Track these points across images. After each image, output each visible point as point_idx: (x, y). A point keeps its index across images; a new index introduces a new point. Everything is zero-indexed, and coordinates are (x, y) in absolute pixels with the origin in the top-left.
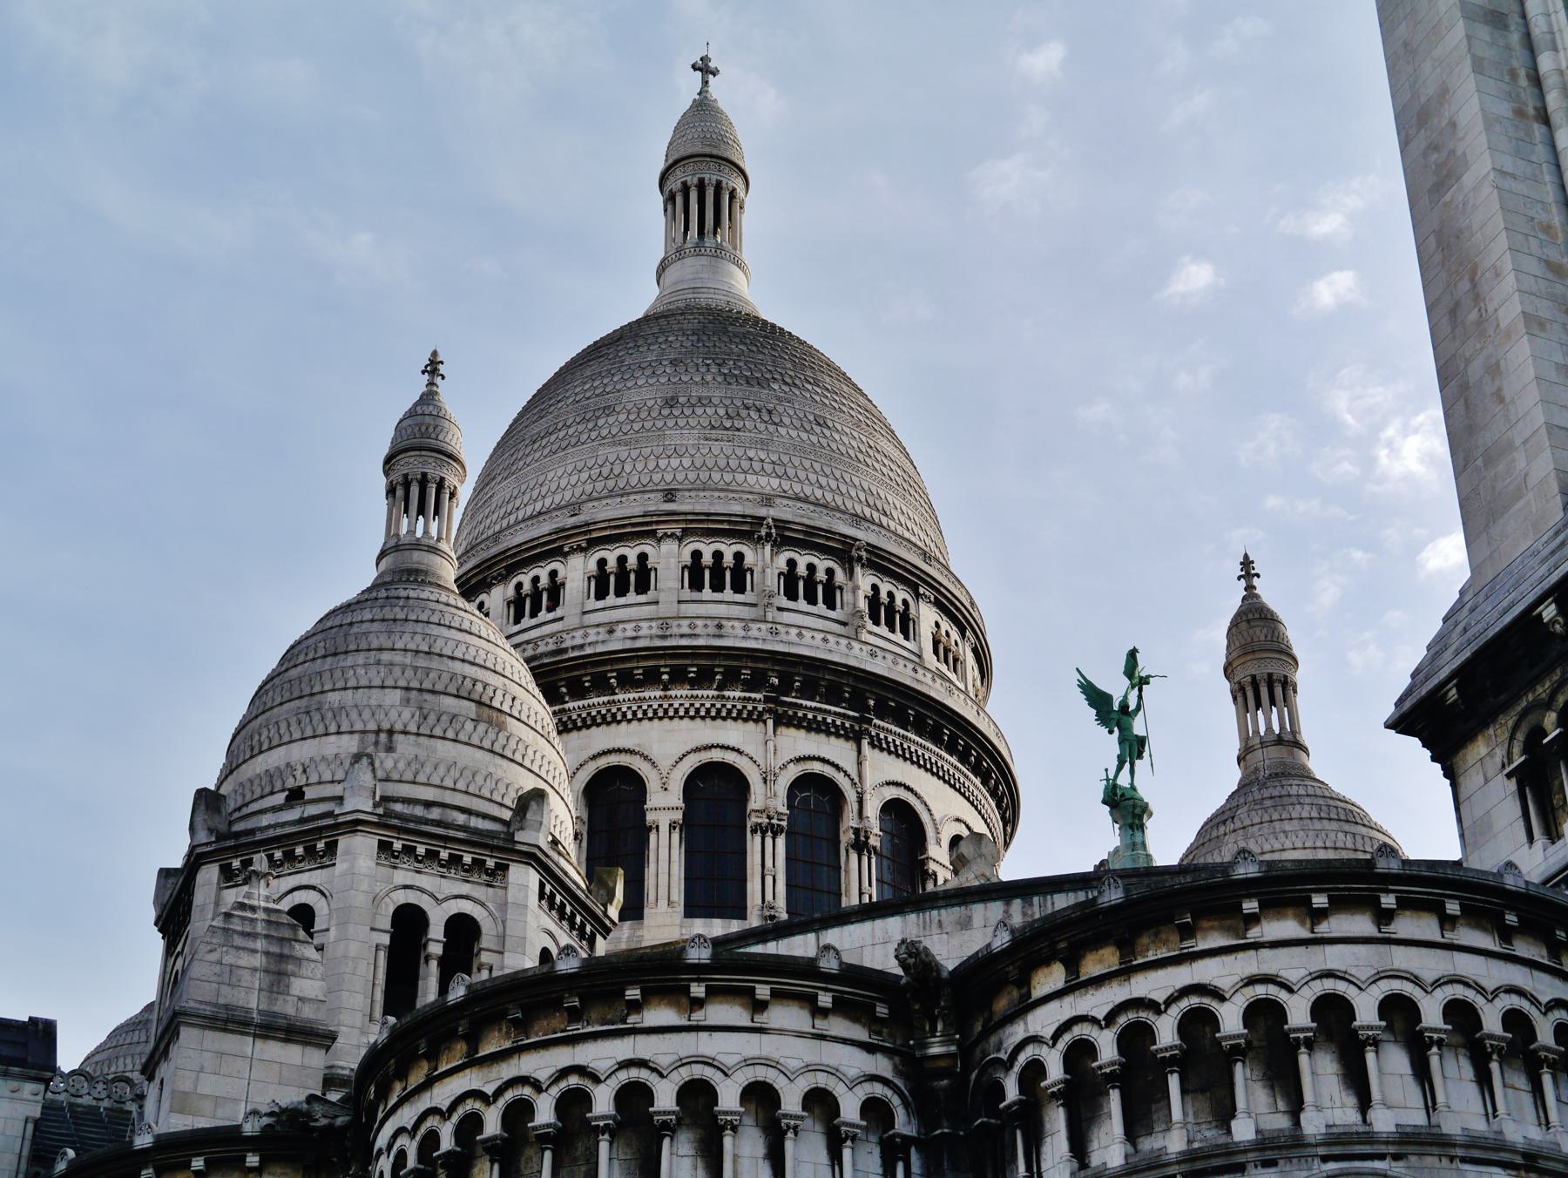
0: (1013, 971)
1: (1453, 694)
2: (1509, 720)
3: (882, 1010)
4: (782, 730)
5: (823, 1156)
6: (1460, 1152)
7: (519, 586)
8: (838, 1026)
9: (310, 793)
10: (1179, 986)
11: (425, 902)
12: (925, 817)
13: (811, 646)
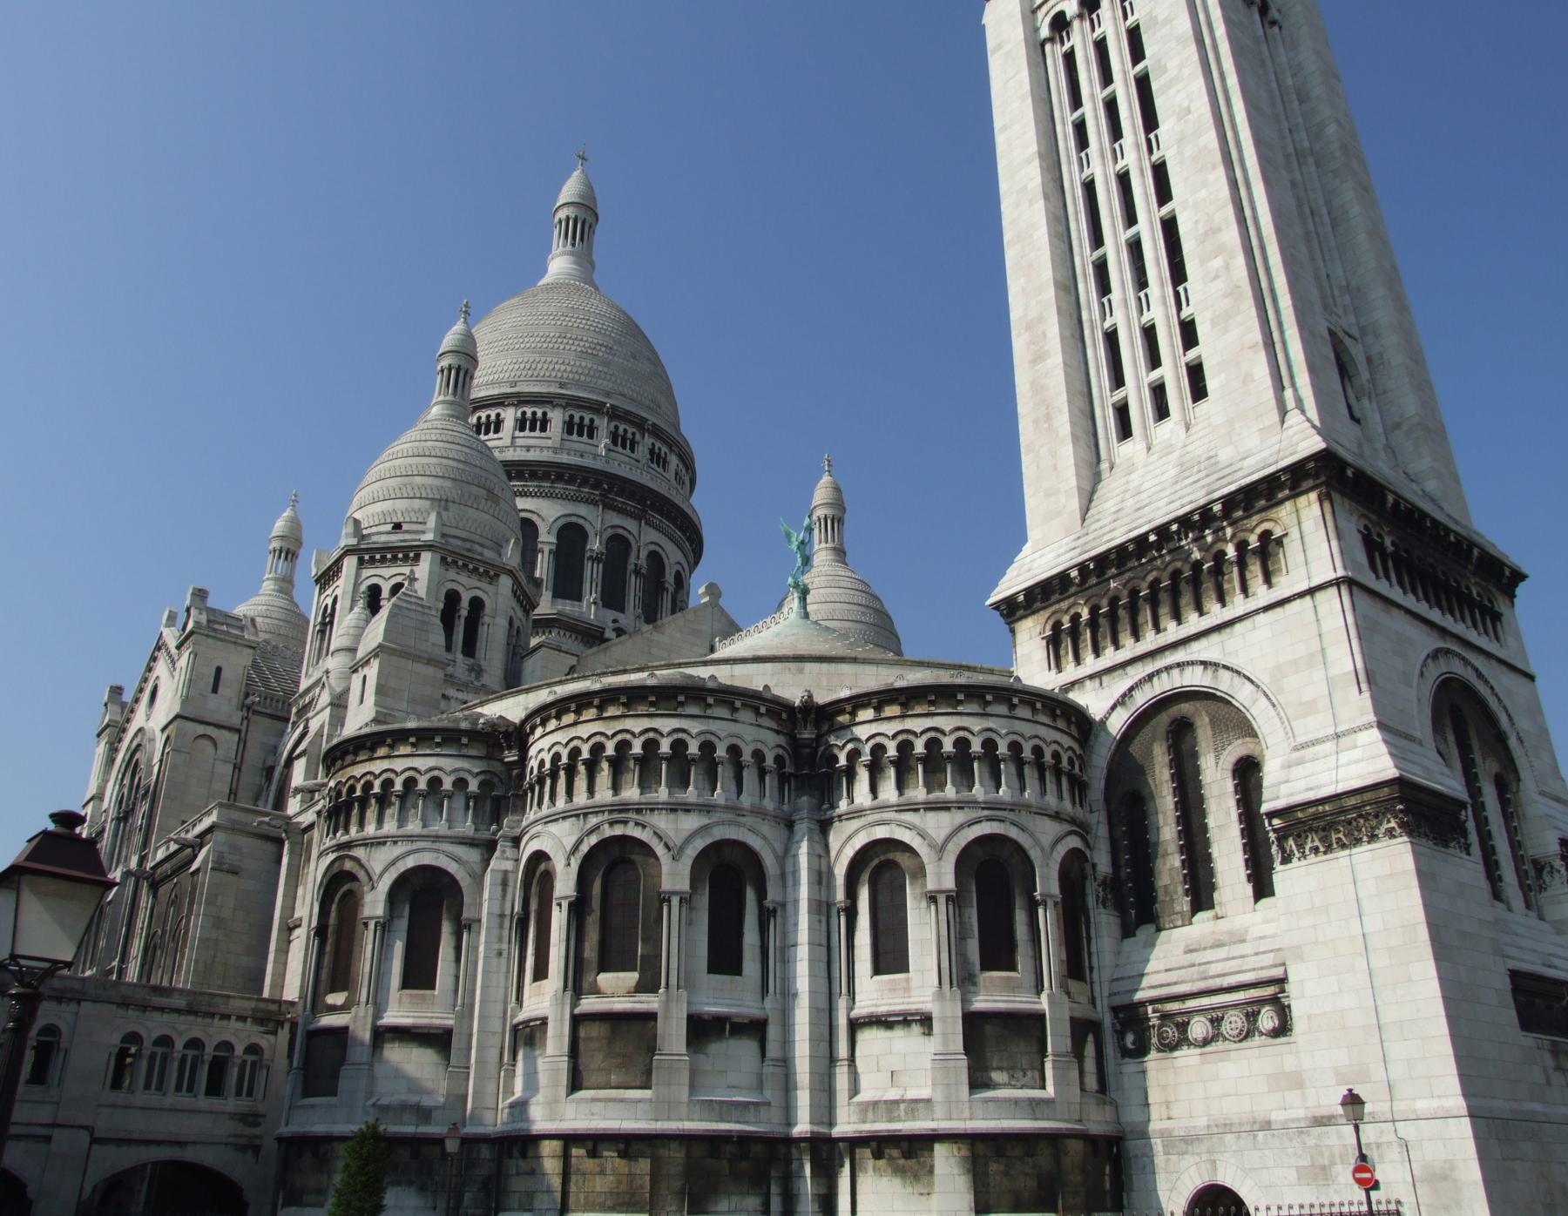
0: (849, 708)
1: (1021, 598)
2: (1045, 614)
3: (784, 716)
4: (606, 510)
5: (756, 778)
6: (1034, 810)
7: (479, 418)
8: (767, 722)
9: (405, 527)
10: (927, 726)
11: (460, 589)
12: (666, 560)
13: (623, 471)
